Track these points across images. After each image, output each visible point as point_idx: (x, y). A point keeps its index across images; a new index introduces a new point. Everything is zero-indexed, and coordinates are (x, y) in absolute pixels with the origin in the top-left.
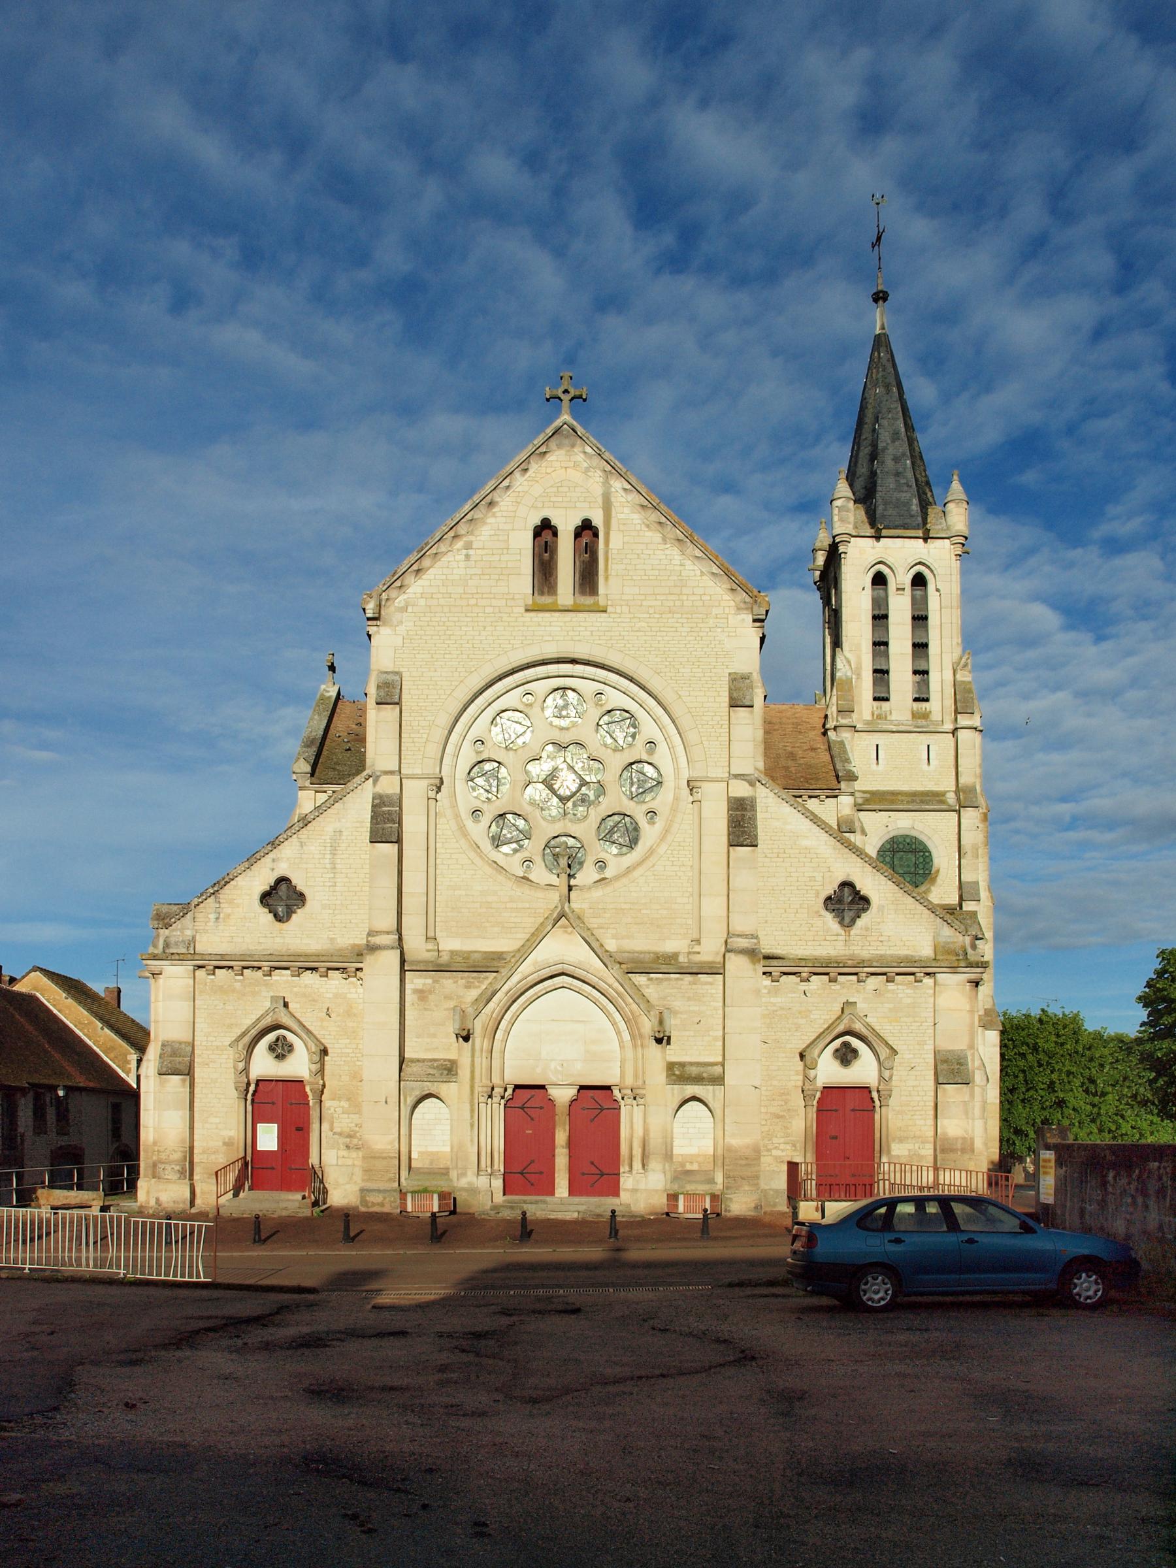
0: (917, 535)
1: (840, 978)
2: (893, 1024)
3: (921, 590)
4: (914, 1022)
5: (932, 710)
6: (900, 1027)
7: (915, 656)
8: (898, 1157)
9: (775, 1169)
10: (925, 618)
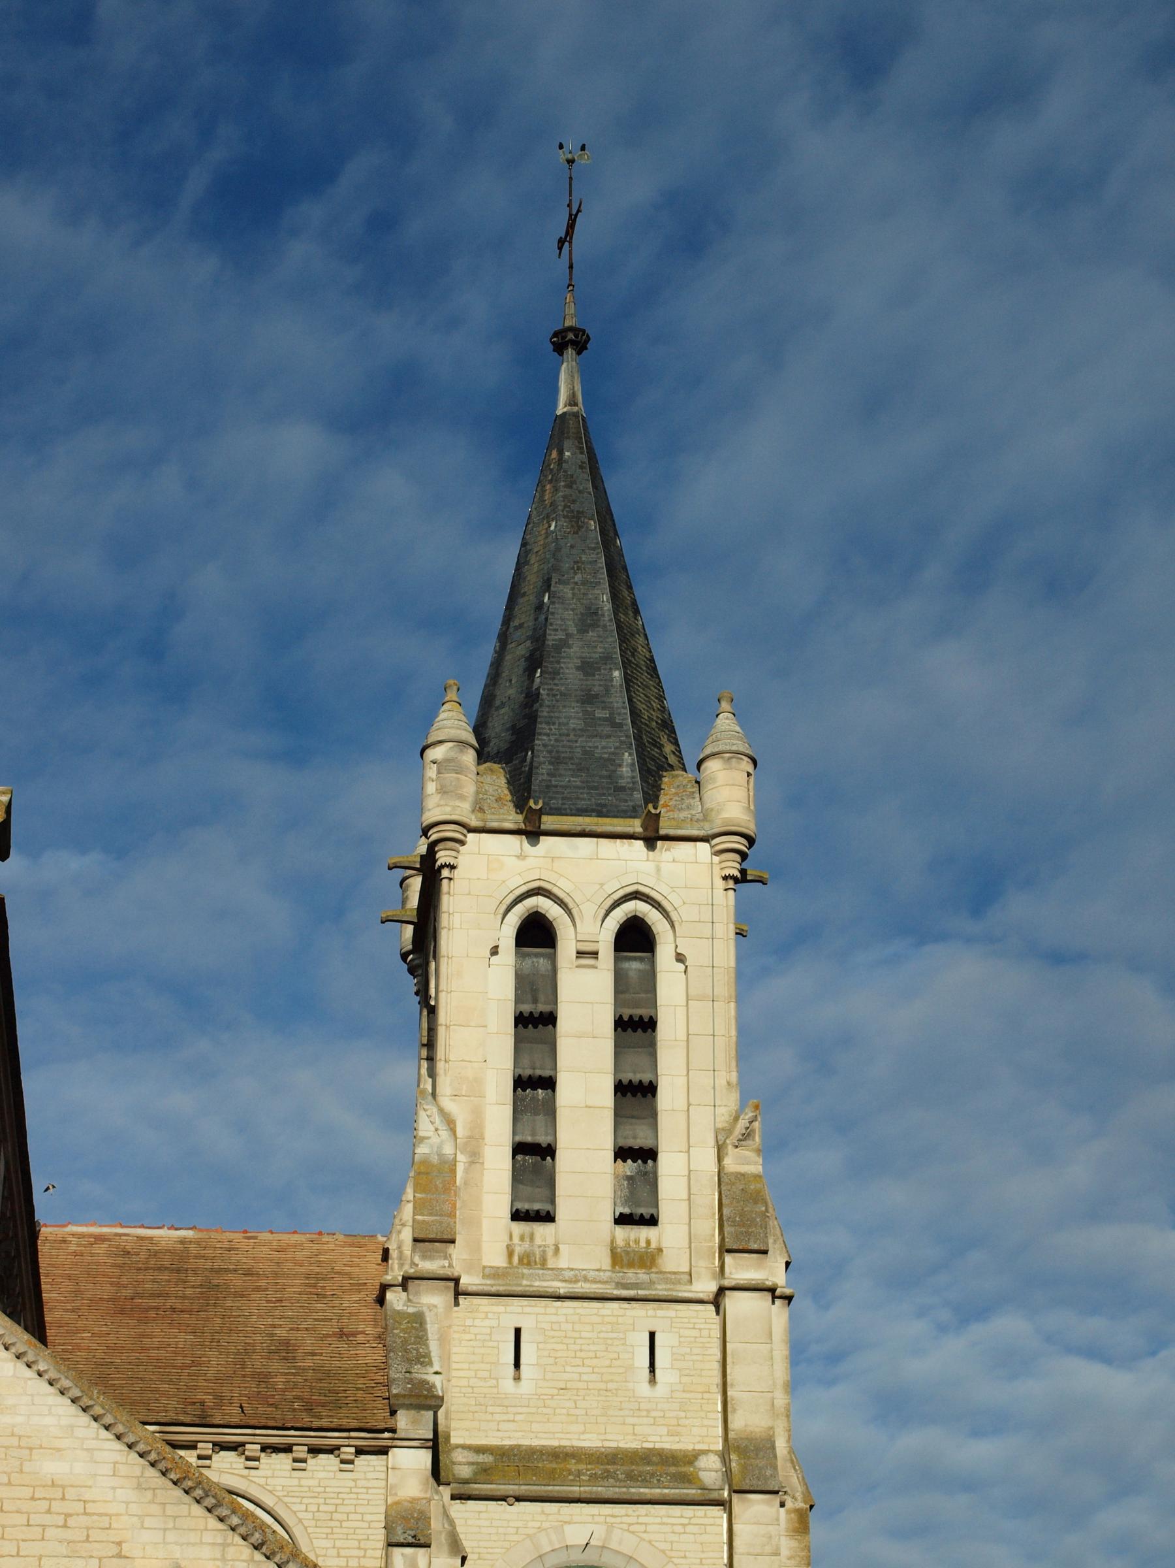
0: (630, 830)
3: (641, 959)
5: (664, 1245)
7: (620, 1115)
10: (650, 1025)
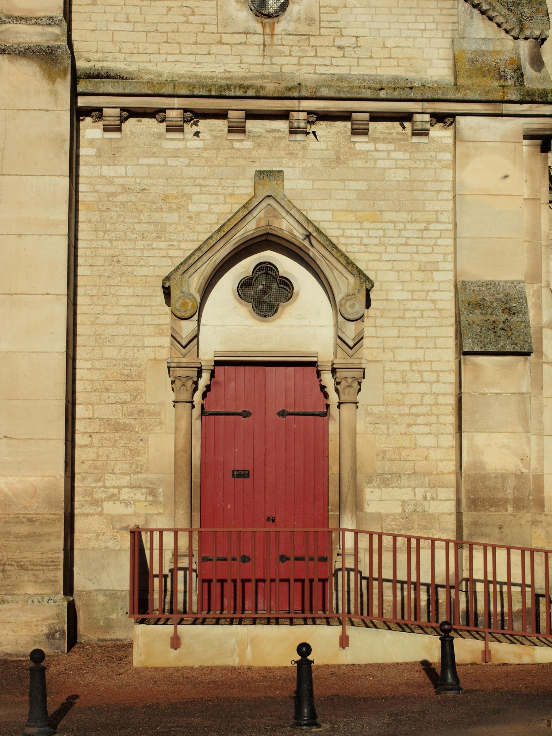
1: (250, 125)
2: (366, 225)
4: (413, 221)
6: (381, 233)
8: (379, 517)
9: (110, 544)
